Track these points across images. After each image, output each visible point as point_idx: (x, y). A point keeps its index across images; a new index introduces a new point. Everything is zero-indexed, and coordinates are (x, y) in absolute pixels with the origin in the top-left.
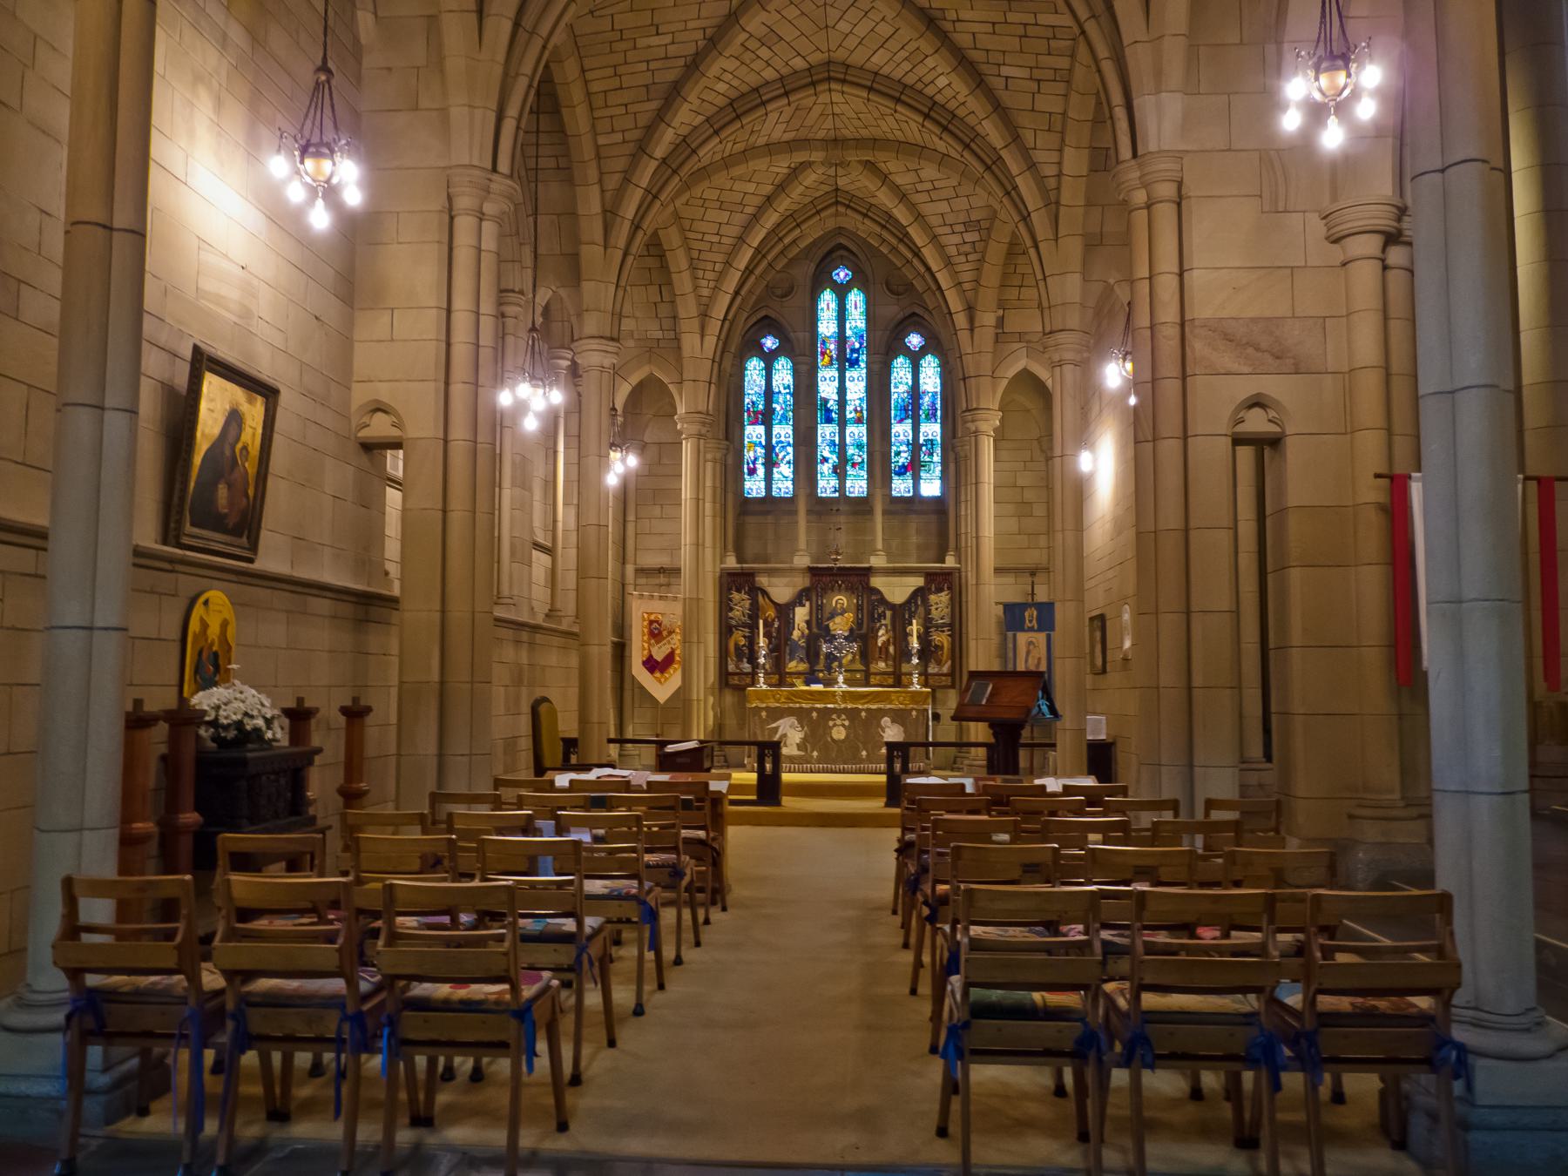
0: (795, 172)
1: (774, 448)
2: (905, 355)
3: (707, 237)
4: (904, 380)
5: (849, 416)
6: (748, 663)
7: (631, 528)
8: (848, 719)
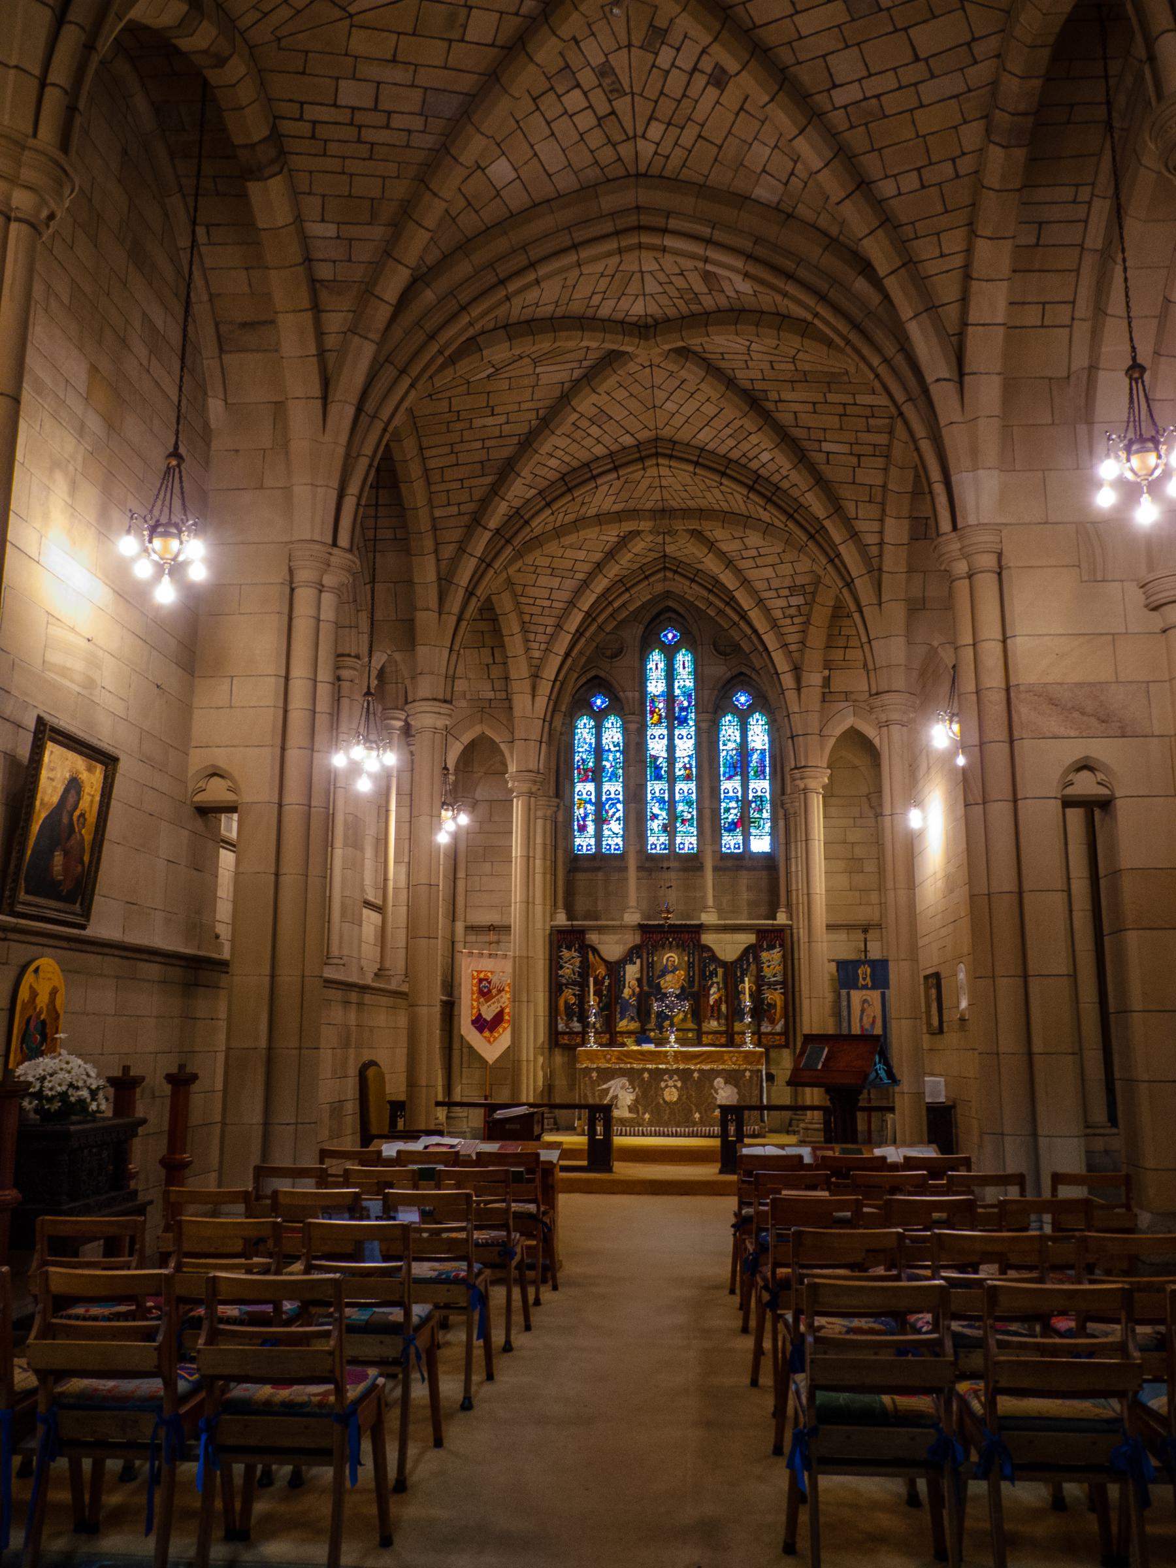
0: (624, 541)
1: (604, 804)
2: (733, 714)
3: (538, 602)
4: (733, 738)
5: (678, 773)
7: (461, 884)
8: (680, 1079)
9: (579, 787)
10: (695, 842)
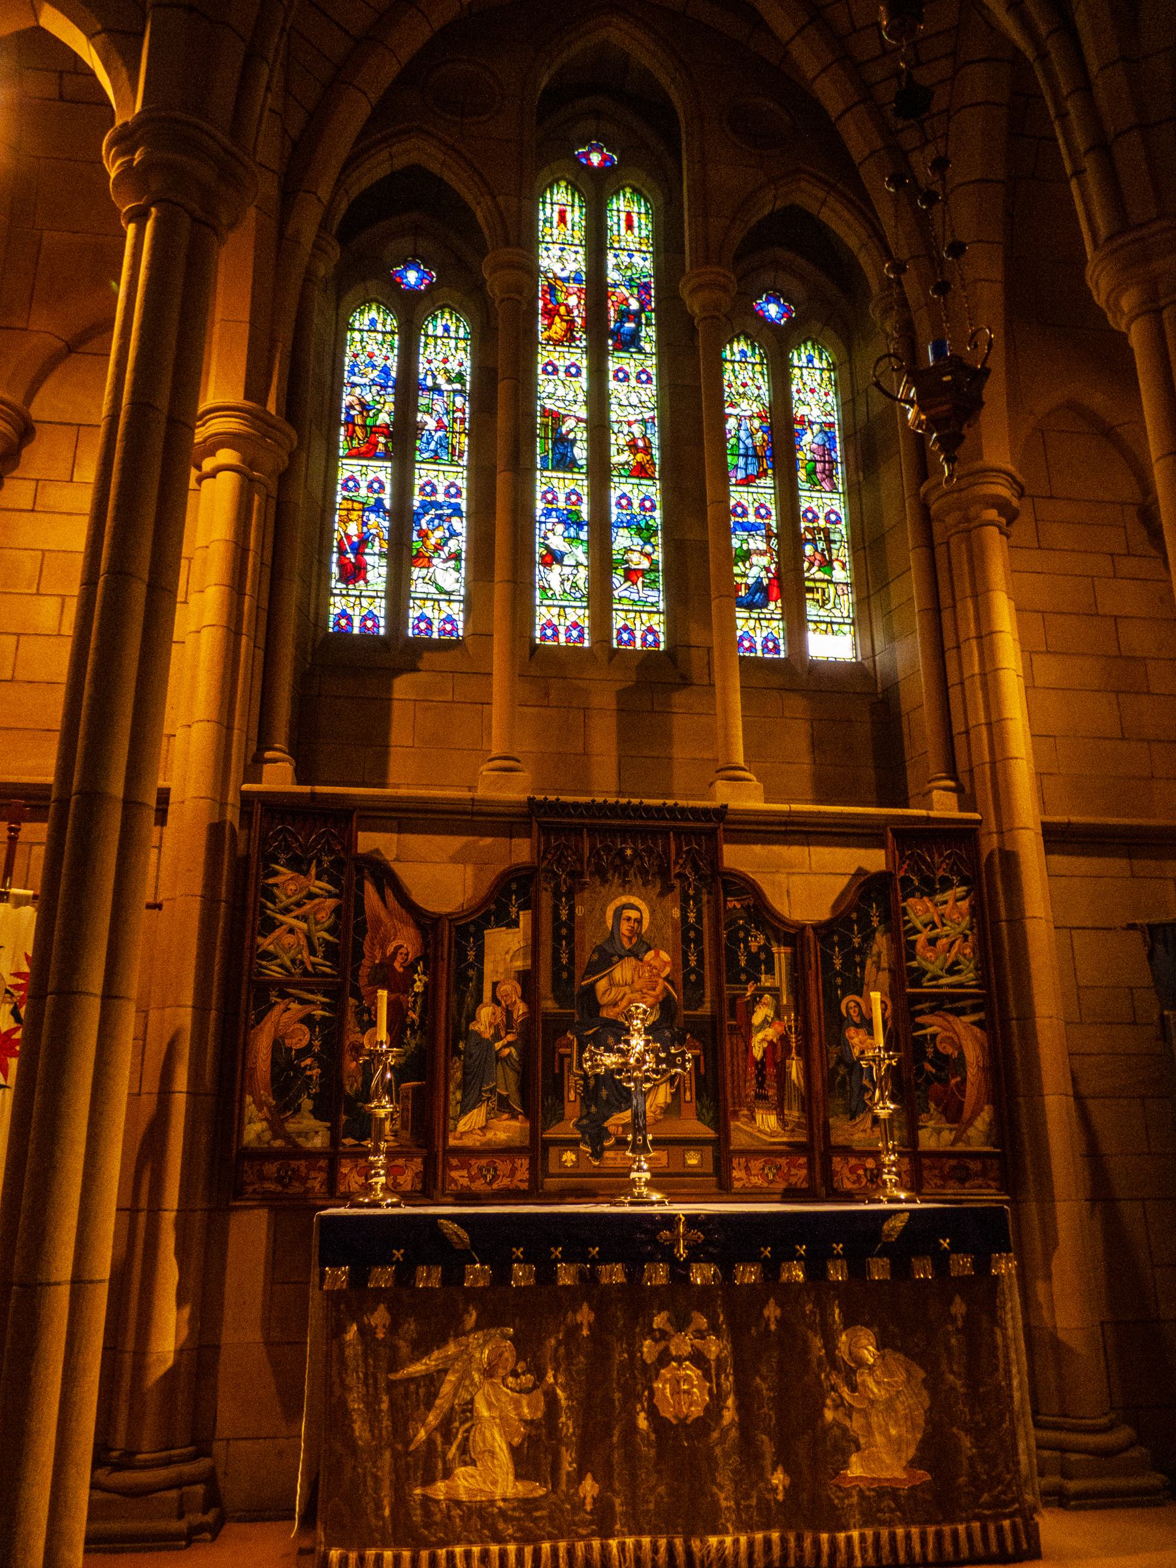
1: (418, 516)
5: (616, 459)
6: (317, 1113)
9: (348, 468)
10: (661, 629)
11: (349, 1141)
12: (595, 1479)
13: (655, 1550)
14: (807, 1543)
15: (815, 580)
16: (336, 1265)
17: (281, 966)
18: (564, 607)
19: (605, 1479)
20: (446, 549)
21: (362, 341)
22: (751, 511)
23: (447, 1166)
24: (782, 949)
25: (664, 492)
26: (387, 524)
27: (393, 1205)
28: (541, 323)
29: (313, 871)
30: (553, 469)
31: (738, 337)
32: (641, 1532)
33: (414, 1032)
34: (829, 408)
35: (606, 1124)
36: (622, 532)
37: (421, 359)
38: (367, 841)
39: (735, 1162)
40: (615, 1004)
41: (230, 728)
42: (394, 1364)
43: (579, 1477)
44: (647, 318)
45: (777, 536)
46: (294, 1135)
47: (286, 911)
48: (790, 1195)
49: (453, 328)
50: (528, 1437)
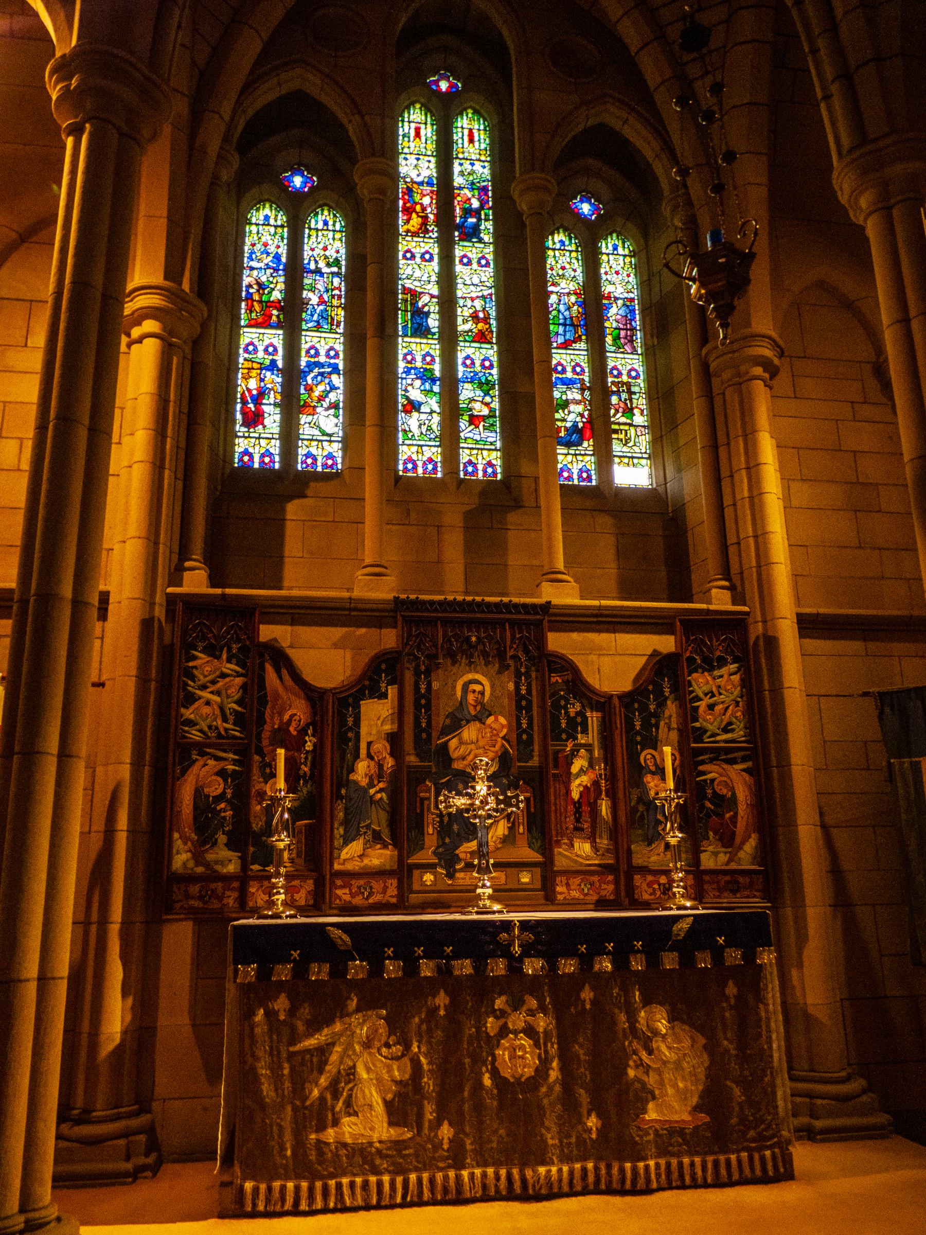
1: (305, 374)
5: (462, 327)
6: (230, 846)
9: (248, 335)
11: (256, 867)
12: (450, 1124)
13: (497, 1178)
14: (615, 1170)
15: (619, 424)
16: (246, 963)
17: (201, 731)
18: (421, 446)
19: (458, 1124)
20: (327, 400)
21: (258, 233)
22: (569, 369)
23: (333, 884)
24: (595, 714)
25: (500, 354)
26: (280, 380)
27: (291, 916)
28: (402, 218)
29: (224, 656)
30: (411, 337)
31: (558, 229)
32: (486, 1165)
33: (306, 782)
34: (630, 287)
35: (457, 852)
36: (466, 385)
37: (306, 247)
38: (267, 632)
39: (558, 880)
40: (464, 758)
41: (156, 543)
42: (293, 1041)
43: (438, 1123)
44: (486, 215)
45: (589, 388)
46: (212, 864)
47: (204, 687)
48: (601, 904)
49: (331, 223)
50: (398, 1094)
